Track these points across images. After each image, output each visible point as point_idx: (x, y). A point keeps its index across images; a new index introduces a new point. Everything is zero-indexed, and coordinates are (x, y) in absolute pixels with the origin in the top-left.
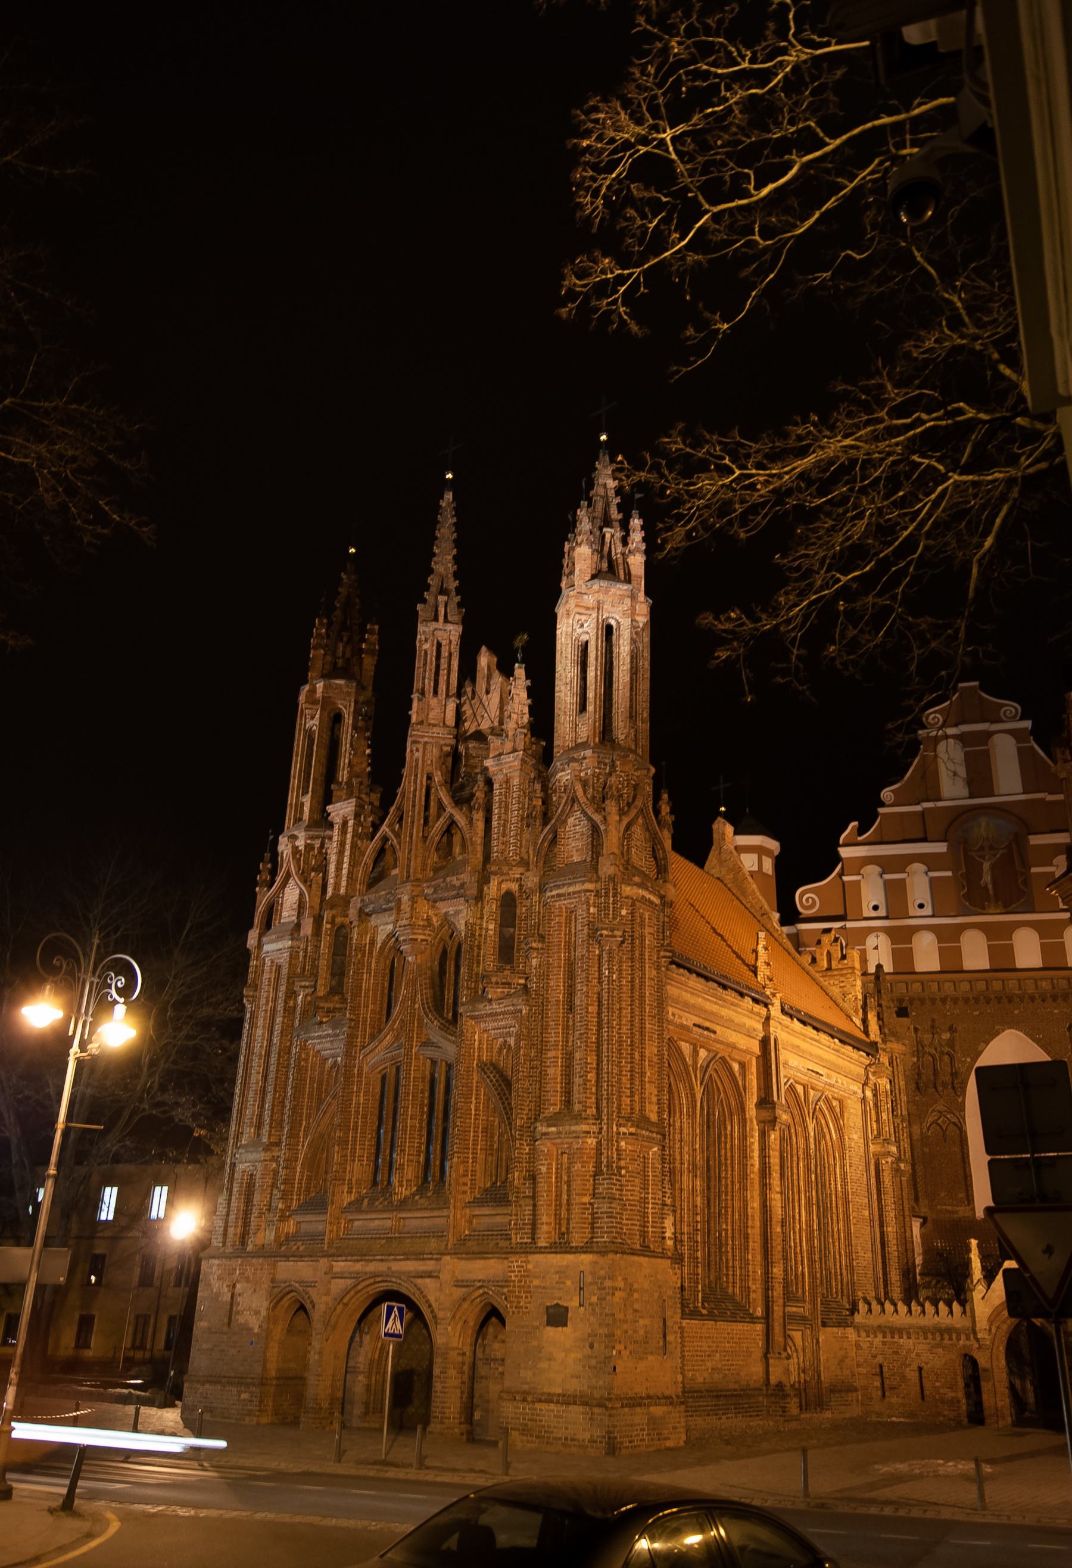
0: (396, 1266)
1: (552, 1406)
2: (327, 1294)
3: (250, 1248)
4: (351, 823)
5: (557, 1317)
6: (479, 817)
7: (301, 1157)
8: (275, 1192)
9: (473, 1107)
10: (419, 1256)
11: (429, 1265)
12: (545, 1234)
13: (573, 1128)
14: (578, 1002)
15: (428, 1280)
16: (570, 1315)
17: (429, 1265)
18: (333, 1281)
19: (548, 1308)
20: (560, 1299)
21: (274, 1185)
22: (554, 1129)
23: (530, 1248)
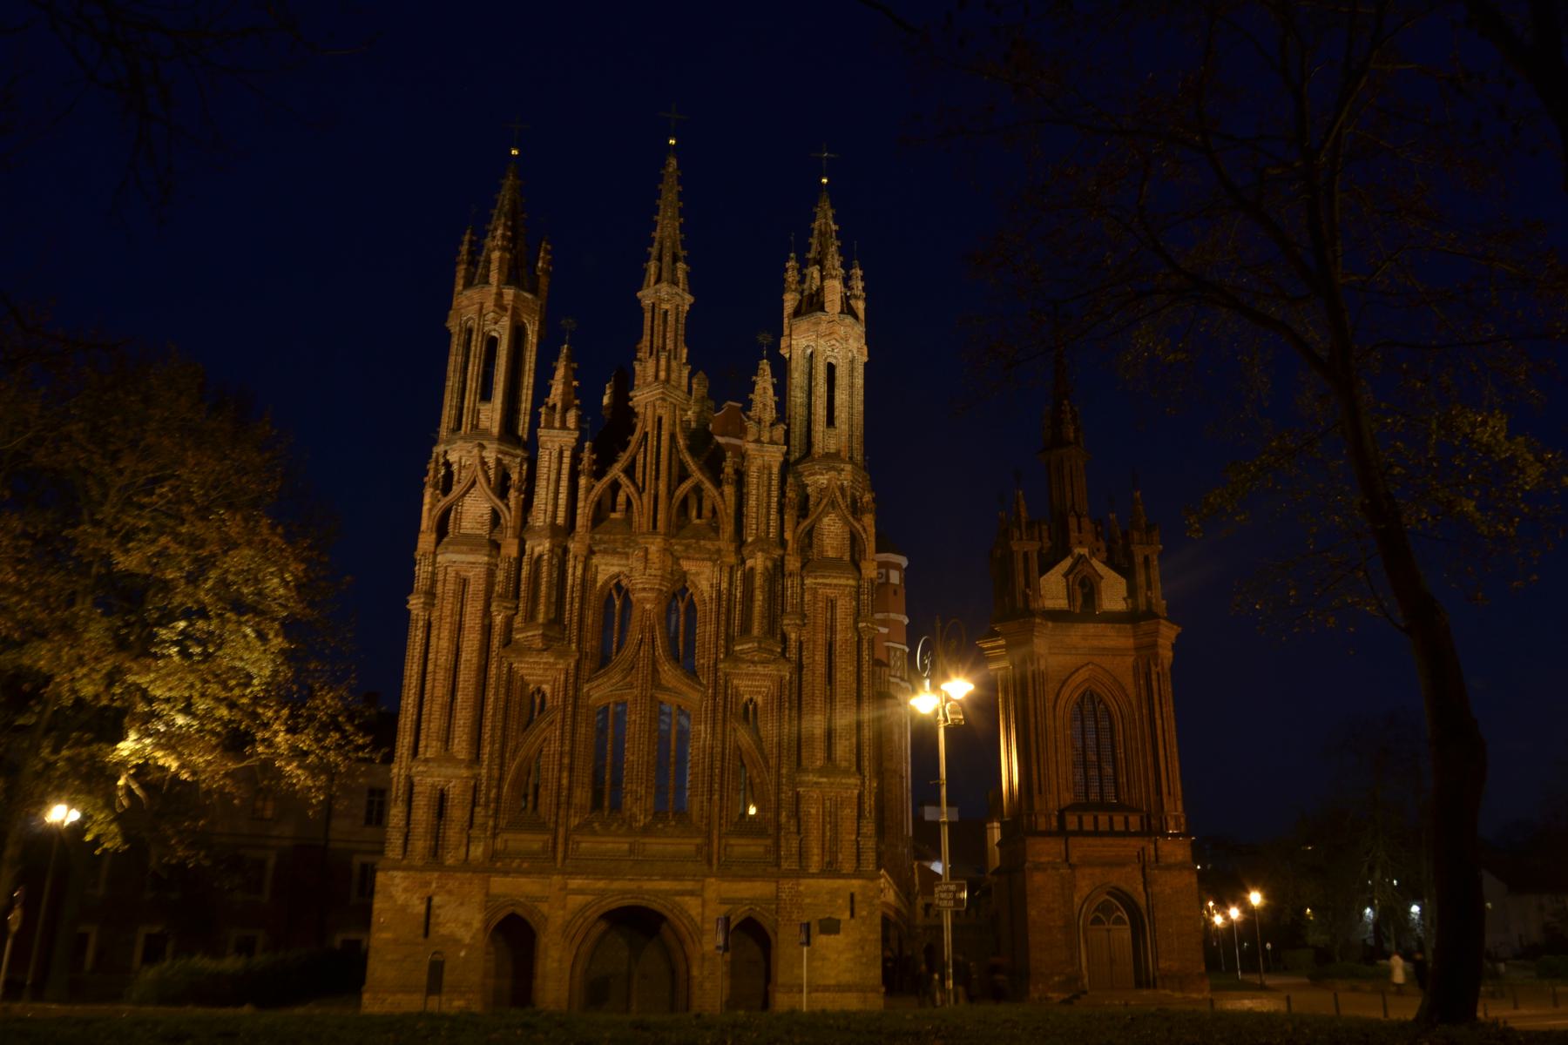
0: (647, 885)
1: (827, 994)
2: (564, 907)
3: (450, 860)
4: (567, 454)
5: (830, 927)
6: (729, 490)
7: (509, 778)
8: (478, 809)
9: (727, 751)
10: (677, 877)
11: (689, 885)
12: (815, 862)
13: (844, 781)
14: (839, 676)
15: (687, 898)
16: (841, 926)
17: (689, 885)
18: (569, 897)
19: (820, 921)
20: (832, 913)
21: (474, 803)
22: (824, 780)
23: (802, 872)
